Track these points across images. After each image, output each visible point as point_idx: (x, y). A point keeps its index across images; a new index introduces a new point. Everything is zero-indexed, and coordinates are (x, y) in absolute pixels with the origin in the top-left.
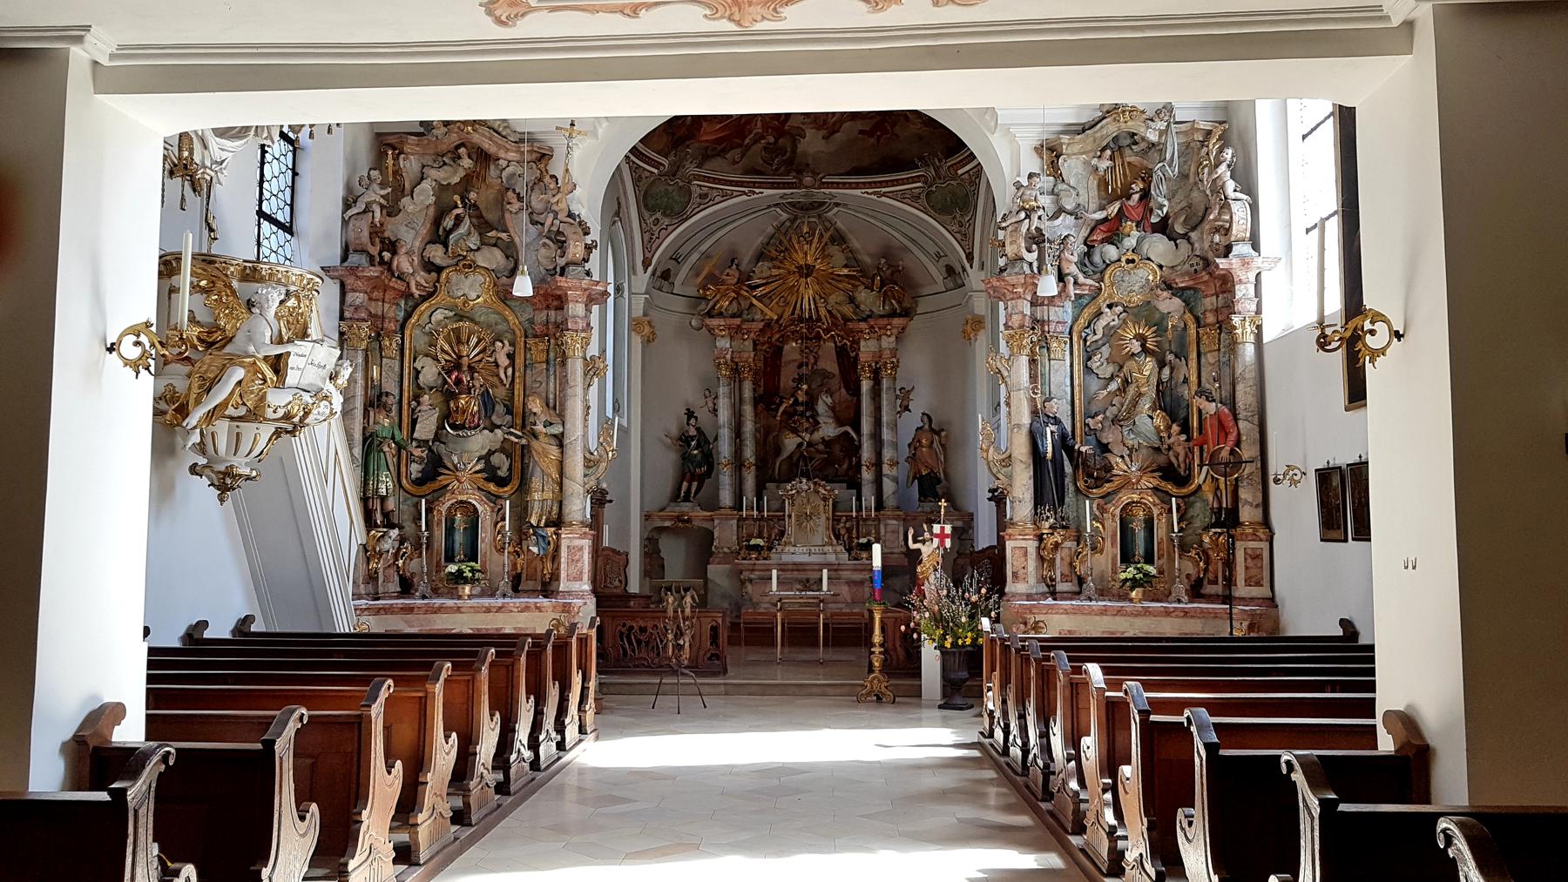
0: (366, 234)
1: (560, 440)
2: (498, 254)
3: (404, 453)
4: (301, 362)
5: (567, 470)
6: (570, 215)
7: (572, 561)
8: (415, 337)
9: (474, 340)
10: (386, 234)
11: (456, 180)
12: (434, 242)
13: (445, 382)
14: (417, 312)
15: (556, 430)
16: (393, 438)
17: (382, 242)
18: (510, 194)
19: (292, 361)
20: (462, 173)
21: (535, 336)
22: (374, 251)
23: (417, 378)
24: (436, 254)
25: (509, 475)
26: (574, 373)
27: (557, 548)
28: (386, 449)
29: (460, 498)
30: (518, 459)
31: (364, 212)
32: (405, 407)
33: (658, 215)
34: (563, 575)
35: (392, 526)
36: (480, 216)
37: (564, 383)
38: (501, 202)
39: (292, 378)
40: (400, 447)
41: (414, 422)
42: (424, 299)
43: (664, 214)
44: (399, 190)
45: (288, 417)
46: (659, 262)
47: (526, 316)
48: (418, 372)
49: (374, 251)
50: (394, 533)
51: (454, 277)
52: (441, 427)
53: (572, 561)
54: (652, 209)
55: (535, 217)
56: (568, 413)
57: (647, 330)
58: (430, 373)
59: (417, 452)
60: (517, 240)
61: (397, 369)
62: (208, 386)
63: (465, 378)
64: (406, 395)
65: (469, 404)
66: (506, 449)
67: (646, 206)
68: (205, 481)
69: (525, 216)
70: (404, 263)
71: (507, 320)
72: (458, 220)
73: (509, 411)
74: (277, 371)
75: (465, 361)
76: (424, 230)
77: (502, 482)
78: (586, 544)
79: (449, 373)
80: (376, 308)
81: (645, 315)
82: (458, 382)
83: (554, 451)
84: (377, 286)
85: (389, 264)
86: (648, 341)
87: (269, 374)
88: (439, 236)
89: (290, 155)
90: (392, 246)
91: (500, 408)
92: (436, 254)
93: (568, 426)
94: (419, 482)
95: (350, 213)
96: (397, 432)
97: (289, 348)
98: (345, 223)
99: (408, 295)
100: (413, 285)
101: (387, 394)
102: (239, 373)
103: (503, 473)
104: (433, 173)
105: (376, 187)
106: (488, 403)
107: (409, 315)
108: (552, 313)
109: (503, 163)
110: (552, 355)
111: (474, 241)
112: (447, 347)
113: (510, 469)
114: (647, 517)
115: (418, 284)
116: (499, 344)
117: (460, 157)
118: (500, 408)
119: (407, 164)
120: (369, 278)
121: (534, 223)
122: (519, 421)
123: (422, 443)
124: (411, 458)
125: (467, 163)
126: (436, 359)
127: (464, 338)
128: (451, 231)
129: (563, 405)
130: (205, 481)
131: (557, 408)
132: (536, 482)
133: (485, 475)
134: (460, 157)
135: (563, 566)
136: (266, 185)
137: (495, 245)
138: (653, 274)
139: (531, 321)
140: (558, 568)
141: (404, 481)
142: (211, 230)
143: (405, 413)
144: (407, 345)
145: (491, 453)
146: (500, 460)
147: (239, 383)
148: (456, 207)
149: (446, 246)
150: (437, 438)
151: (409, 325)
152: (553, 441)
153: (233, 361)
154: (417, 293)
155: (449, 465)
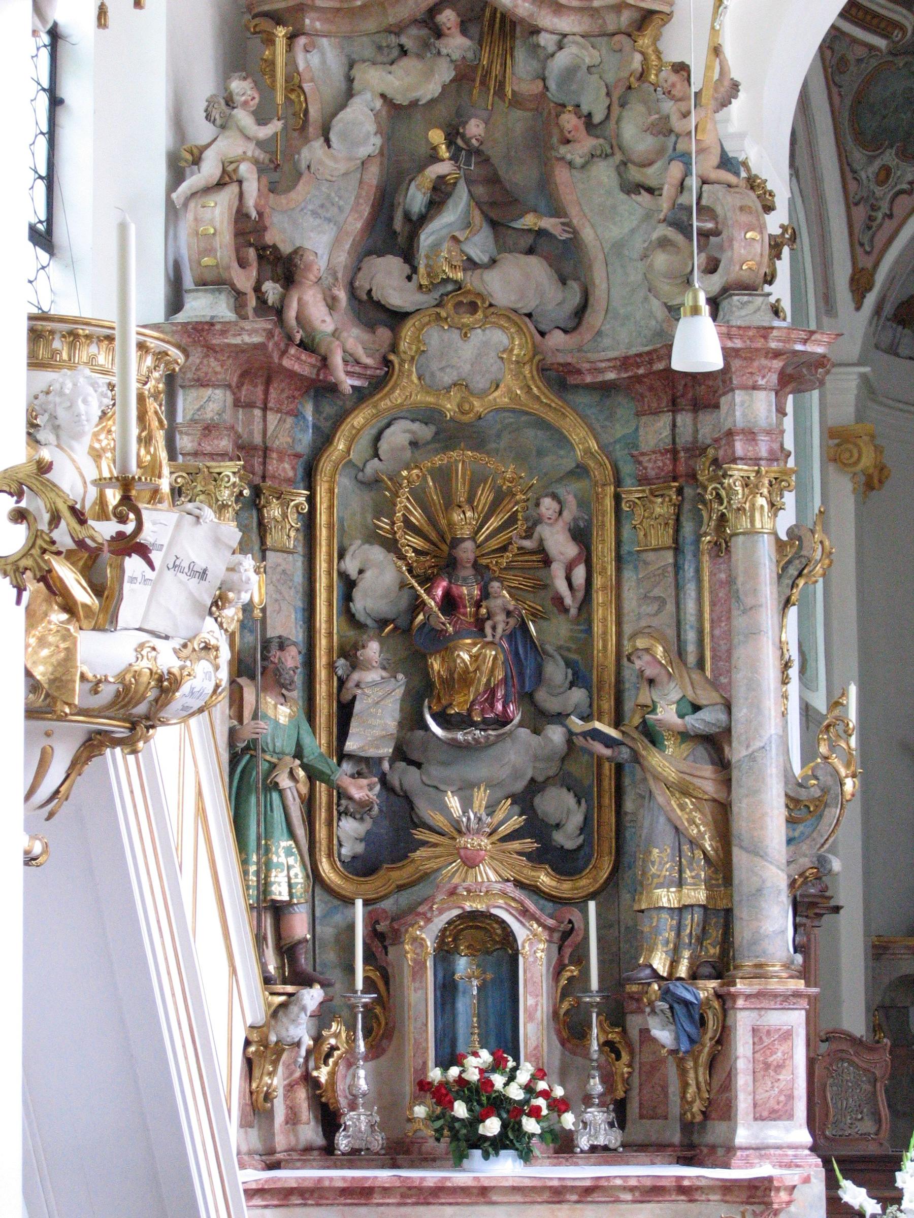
0: (225, 239)
1: (715, 745)
2: (536, 269)
3: (322, 788)
5: (741, 824)
6: (726, 162)
7: (765, 1068)
8: (337, 496)
9: (484, 497)
10: (270, 238)
11: (431, 89)
12: (380, 254)
13: (417, 605)
14: (345, 430)
15: (707, 719)
16: (299, 754)
17: (260, 258)
18: (569, 121)
20: (444, 73)
21: (643, 480)
22: (244, 280)
23: (347, 598)
24: (389, 280)
25: (584, 841)
26: (752, 572)
27: (723, 1038)
28: (285, 782)
29: (468, 906)
30: (608, 800)
31: (220, 185)
32: (322, 674)
33: (889, 157)
34: (743, 1103)
35: (306, 981)
36: (494, 180)
37: (730, 596)
38: (543, 142)
40: (313, 775)
41: (345, 713)
42: (361, 396)
43: (904, 155)
44: (300, 123)
45: (125, 696)
46: (891, 280)
47: (620, 430)
48: (349, 585)
49: (244, 280)
50: (313, 997)
51: (435, 337)
52: (412, 720)
53: (765, 1068)
54: (872, 143)
55: (635, 174)
56: (740, 677)
57: (867, 460)
58: (380, 580)
59: (362, 790)
60: (587, 234)
61: (299, 577)
63: (468, 591)
64: (322, 643)
65: (476, 657)
66: (569, 769)
67: (860, 137)
69: (604, 173)
70: (316, 308)
71: (562, 440)
72: (440, 194)
73: (579, 678)
74: (98, 590)
75: (466, 552)
76: (356, 225)
77: (565, 863)
78: (795, 1020)
79: (427, 581)
80: (252, 425)
81: (860, 416)
82: (450, 604)
83: (706, 780)
84: (256, 374)
85: (279, 312)
86: (871, 484)
87: (82, 595)
88: (391, 231)
90: (285, 268)
91: (556, 672)
92: (389, 280)
93: (740, 713)
94: (362, 867)
95: (185, 188)
96: (308, 740)
98: (173, 212)
99: (322, 389)
100: (337, 360)
101: (282, 645)
103: (567, 838)
104: (376, 79)
105: (243, 118)
106: (524, 649)
107: (324, 440)
108: (684, 419)
109: (546, 40)
110: (688, 528)
111: (479, 246)
112: (417, 517)
113: (585, 828)
114: (879, 951)
115: (351, 359)
116: (548, 506)
117: (438, 33)
118: (556, 672)
119: (314, 59)
120: (238, 351)
121: (633, 188)
122: (608, 705)
123: (366, 765)
124: (342, 804)
125: (457, 44)
126: (391, 545)
127: (461, 491)
128: (423, 219)
129: (725, 658)
131: (711, 661)
132: (660, 859)
133: (528, 844)
134: (438, 33)
135: (743, 1081)
137: (530, 251)
138: (878, 310)
139: (631, 442)
140: (728, 1085)
141: (325, 867)
143: (322, 690)
144: (322, 518)
145: (534, 787)
146: (560, 804)
148: (434, 158)
149: (408, 255)
150: (401, 754)
151: (326, 466)
152: (701, 751)
154: (348, 383)
155: (439, 820)
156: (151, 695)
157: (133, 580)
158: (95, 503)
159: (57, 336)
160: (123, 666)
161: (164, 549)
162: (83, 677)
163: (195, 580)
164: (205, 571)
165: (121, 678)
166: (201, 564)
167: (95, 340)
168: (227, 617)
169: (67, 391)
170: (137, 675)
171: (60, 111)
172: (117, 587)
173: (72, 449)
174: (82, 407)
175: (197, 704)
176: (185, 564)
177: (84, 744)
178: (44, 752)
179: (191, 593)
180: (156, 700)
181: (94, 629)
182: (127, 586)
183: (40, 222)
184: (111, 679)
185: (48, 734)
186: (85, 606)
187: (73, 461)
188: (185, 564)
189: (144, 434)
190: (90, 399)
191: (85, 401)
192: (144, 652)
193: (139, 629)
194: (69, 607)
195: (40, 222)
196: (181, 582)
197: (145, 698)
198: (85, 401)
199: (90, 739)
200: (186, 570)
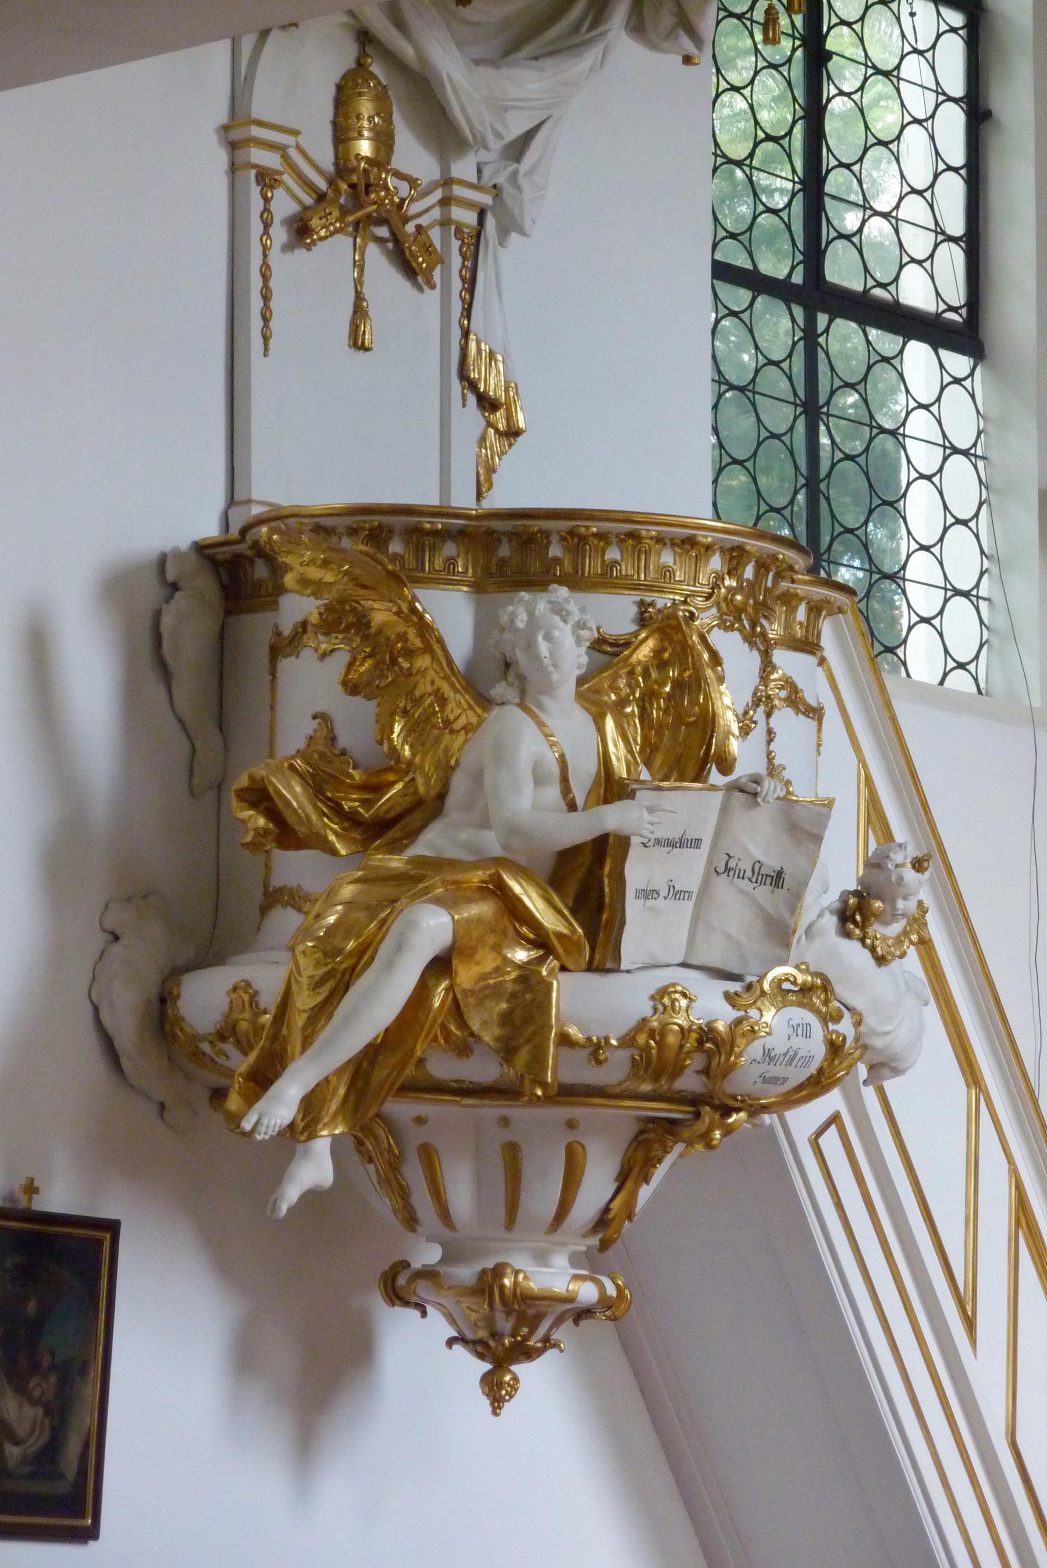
19: (638, 872)
39: (651, 929)
62: (341, 974)
89: (953, 53)
97: (614, 817)
102: (431, 927)
130: (437, 1326)
142: (488, 404)
147: (440, 965)
153: (413, 882)
156: (697, 1062)
157: (648, 894)
158: (596, 783)
159: (555, 539)
160: (632, 1022)
162: (565, 1040)
164: (780, 874)
165: (628, 1041)
166: (772, 863)
167: (614, 539)
168: (885, 938)
170: (659, 1035)
171: (985, 128)
172: (619, 906)
173: (540, 706)
174: (543, 647)
175: (799, 1075)
176: (746, 865)
177: (636, 1137)
179: (761, 908)
180: (706, 1071)
182: (633, 907)
183: (951, 309)
184: (614, 1042)
185: (571, 1125)
186: (560, 936)
187: (541, 725)
188: (746, 865)
189: (687, 674)
190: (557, 633)
191: (548, 637)
192: (666, 1000)
193: (684, 965)
194: (542, 942)
196: (741, 891)
198: (548, 637)
199: (642, 1132)
200: (749, 874)
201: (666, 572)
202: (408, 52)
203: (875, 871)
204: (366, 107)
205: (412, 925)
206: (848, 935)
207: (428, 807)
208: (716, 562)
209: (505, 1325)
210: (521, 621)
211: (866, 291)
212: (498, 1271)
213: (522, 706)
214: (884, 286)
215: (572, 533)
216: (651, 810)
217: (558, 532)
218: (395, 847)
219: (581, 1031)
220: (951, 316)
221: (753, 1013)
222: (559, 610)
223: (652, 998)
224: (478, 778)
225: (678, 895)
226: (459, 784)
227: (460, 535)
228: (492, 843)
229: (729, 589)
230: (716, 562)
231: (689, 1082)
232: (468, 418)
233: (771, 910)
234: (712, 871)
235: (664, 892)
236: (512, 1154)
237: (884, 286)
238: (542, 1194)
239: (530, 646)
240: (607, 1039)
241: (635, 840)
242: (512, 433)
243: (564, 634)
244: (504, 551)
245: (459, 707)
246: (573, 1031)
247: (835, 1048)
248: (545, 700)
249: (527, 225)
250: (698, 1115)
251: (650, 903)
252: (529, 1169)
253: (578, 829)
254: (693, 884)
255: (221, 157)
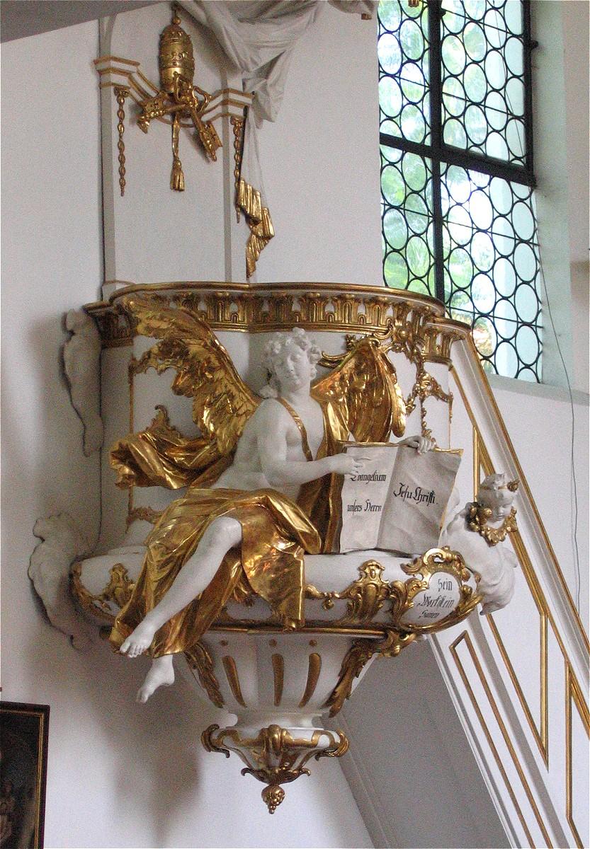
4: (379, 493)
19: (349, 496)
39: (358, 531)
68: (236, 762)
97: (334, 464)
102: (229, 530)
130: (236, 762)
136: (450, 87)
142: (252, 221)
147: (236, 552)
153: (218, 504)
156: (384, 606)
157: (354, 508)
158: (323, 444)
159: (295, 301)
160: (347, 584)
161: (388, 479)
162: (308, 595)
163: (425, 503)
164: (432, 494)
166: (427, 488)
168: (492, 530)
169: (277, 352)
170: (364, 590)
171: (534, 52)
174: (291, 364)
175: (445, 612)
176: (412, 490)
178: (311, 657)
179: (421, 515)
180: (391, 610)
181: (321, 553)
182: (347, 516)
183: (517, 158)
184: (337, 596)
185: (312, 643)
186: (304, 533)
187: (290, 410)
188: (412, 490)
190: (298, 356)
191: (294, 359)
192: (367, 570)
193: (376, 549)
194: (292, 535)
195: (518, 159)
196: (410, 506)
197: (379, 609)
198: (294, 359)
199: (354, 647)
200: (414, 495)
201: (361, 319)
202: (201, 16)
203: (487, 491)
204: (177, 48)
205: (219, 530)
206: (472, 529)
207: (226, 460)
208: (390, 312)
209: (276, 761)
210: (278, 347)
211: (468, 149)
212: (271, 730)
213: (279, 399)
214: (476, 145)
215: (305, 296)
216: (357, 460)
217: (297, 296)
218: (206, 484)
219: (318, 587)
220: (517, 162)
221: (418, 576)
222: (302, 345)
223: (359, 569)
224: (254, 442)
225: (372, 508)
226: (243, 446)
227: (241, 299)
228: (264, 482)
229: (398, 328)
230: (390, 312)
231: (381, 617)
232: (241, 230)
233: (427, 516)
234: (392, 494)
235: (364, 507)
236: (278, 663)
237: (476, 145)
238: (296, 684)
239: (283, 364)
240: (333, 594)
241: (347, 477)
242: (267, 237)
243: (303, 357)
244: (266, 308)
245: (242, 401)
246: (313, 589)
247: (466, 596)
248: (292, 395)
249: (273, 116)
250: (386, 636)
251: (356, 513)
252: (288, 671)
253: (313, 471)
254: (382, 503)
255: (93, 80)
